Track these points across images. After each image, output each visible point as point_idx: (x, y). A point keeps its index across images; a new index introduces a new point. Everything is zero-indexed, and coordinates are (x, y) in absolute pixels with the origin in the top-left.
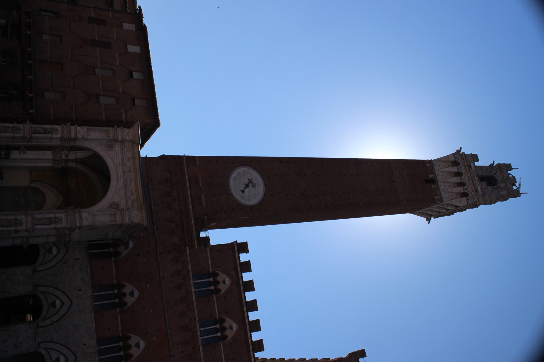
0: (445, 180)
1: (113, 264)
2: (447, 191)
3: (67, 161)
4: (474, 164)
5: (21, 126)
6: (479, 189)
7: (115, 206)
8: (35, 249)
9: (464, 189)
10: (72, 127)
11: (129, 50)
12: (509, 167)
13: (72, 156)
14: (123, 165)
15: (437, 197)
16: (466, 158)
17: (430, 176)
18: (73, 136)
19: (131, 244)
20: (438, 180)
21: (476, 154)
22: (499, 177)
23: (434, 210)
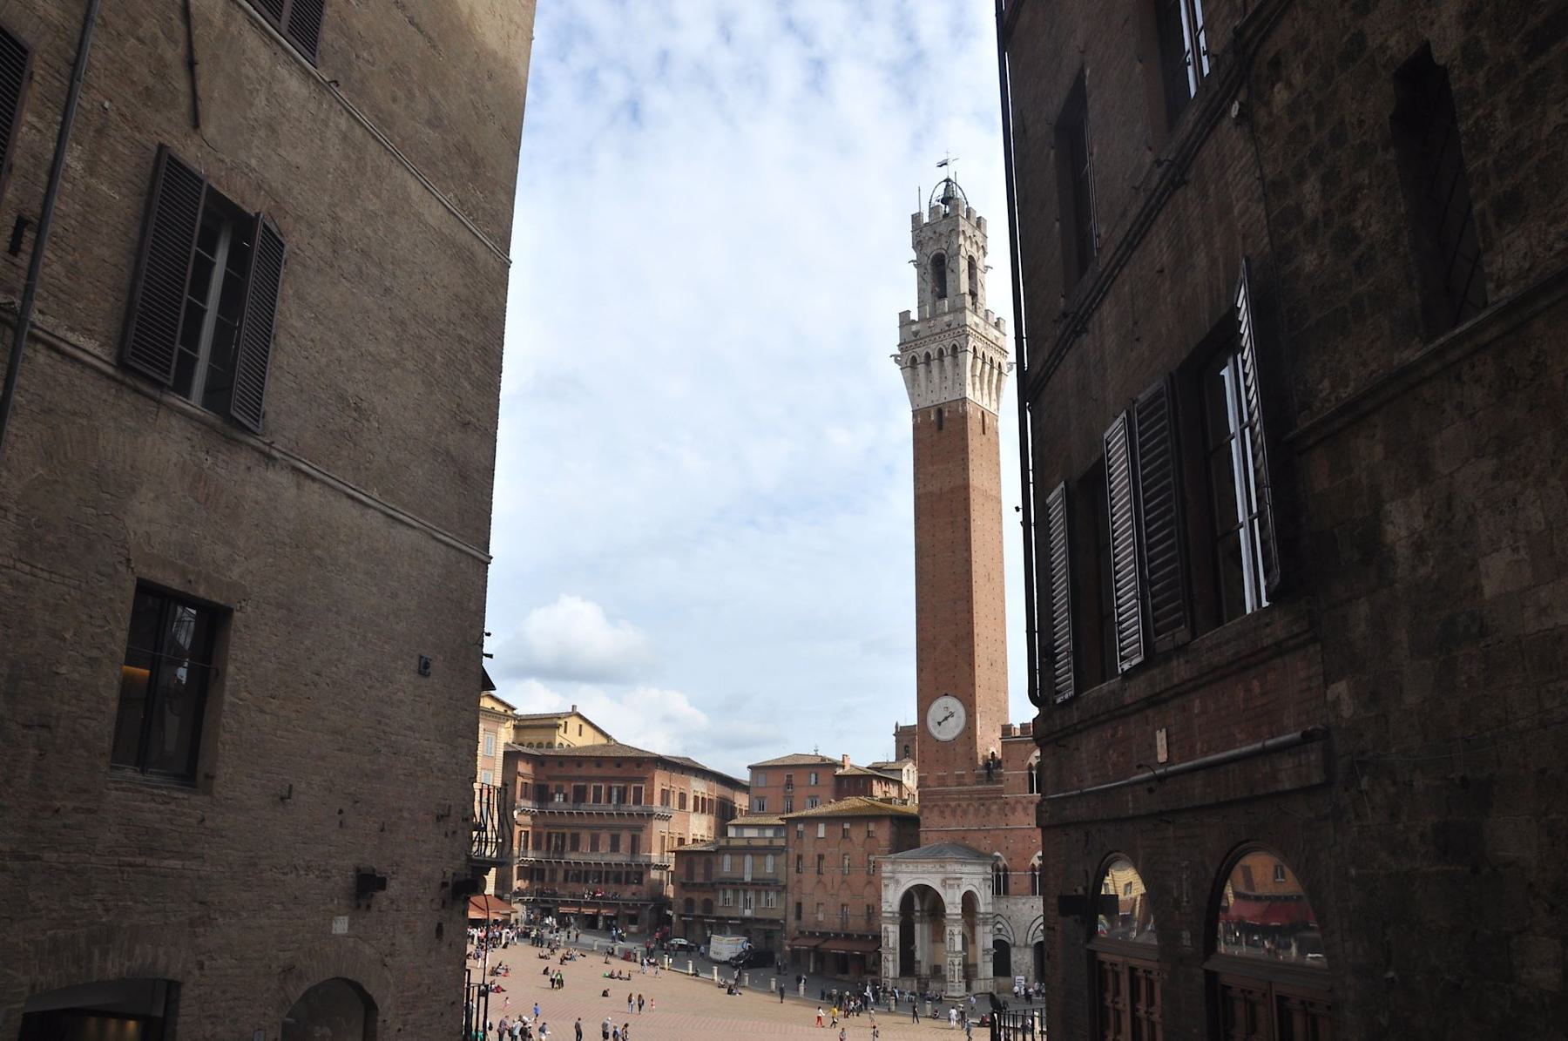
0: (938, 389)
1: (1013, 873)
2: (951, 388)
3: (922, 910)
4: (913, 322)
5: (883, 955)
6: (947, 319)
7: (944, 881)
8: (996, 943)
9: (948, 355)
10: (884, 915)
11: (823, 836)
12: (916, 218)
13: (917, 907)
14: (911, 873)
15: (960, 408)
16: (905, 343)
17: (932, 418)
18: (891, 915)
19: (997, 854)
20: (937, 403)
21: (898, 316)
22: (931, 250)
23: (989, 377)
